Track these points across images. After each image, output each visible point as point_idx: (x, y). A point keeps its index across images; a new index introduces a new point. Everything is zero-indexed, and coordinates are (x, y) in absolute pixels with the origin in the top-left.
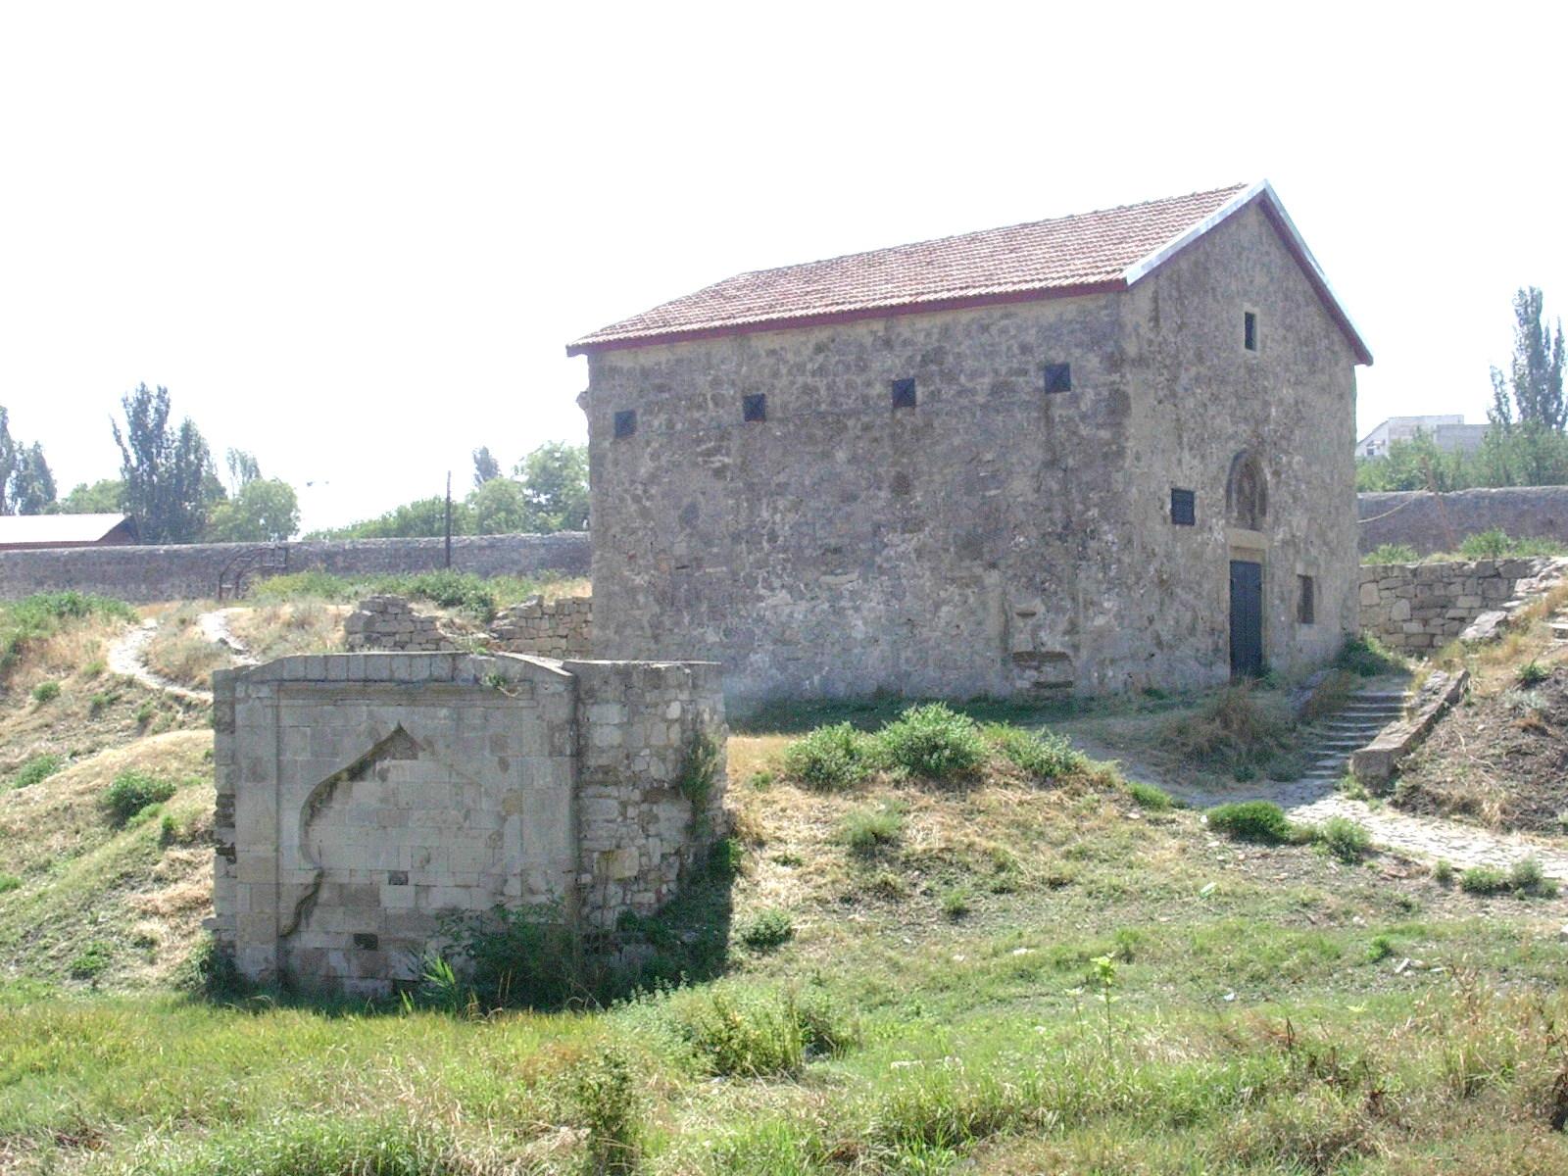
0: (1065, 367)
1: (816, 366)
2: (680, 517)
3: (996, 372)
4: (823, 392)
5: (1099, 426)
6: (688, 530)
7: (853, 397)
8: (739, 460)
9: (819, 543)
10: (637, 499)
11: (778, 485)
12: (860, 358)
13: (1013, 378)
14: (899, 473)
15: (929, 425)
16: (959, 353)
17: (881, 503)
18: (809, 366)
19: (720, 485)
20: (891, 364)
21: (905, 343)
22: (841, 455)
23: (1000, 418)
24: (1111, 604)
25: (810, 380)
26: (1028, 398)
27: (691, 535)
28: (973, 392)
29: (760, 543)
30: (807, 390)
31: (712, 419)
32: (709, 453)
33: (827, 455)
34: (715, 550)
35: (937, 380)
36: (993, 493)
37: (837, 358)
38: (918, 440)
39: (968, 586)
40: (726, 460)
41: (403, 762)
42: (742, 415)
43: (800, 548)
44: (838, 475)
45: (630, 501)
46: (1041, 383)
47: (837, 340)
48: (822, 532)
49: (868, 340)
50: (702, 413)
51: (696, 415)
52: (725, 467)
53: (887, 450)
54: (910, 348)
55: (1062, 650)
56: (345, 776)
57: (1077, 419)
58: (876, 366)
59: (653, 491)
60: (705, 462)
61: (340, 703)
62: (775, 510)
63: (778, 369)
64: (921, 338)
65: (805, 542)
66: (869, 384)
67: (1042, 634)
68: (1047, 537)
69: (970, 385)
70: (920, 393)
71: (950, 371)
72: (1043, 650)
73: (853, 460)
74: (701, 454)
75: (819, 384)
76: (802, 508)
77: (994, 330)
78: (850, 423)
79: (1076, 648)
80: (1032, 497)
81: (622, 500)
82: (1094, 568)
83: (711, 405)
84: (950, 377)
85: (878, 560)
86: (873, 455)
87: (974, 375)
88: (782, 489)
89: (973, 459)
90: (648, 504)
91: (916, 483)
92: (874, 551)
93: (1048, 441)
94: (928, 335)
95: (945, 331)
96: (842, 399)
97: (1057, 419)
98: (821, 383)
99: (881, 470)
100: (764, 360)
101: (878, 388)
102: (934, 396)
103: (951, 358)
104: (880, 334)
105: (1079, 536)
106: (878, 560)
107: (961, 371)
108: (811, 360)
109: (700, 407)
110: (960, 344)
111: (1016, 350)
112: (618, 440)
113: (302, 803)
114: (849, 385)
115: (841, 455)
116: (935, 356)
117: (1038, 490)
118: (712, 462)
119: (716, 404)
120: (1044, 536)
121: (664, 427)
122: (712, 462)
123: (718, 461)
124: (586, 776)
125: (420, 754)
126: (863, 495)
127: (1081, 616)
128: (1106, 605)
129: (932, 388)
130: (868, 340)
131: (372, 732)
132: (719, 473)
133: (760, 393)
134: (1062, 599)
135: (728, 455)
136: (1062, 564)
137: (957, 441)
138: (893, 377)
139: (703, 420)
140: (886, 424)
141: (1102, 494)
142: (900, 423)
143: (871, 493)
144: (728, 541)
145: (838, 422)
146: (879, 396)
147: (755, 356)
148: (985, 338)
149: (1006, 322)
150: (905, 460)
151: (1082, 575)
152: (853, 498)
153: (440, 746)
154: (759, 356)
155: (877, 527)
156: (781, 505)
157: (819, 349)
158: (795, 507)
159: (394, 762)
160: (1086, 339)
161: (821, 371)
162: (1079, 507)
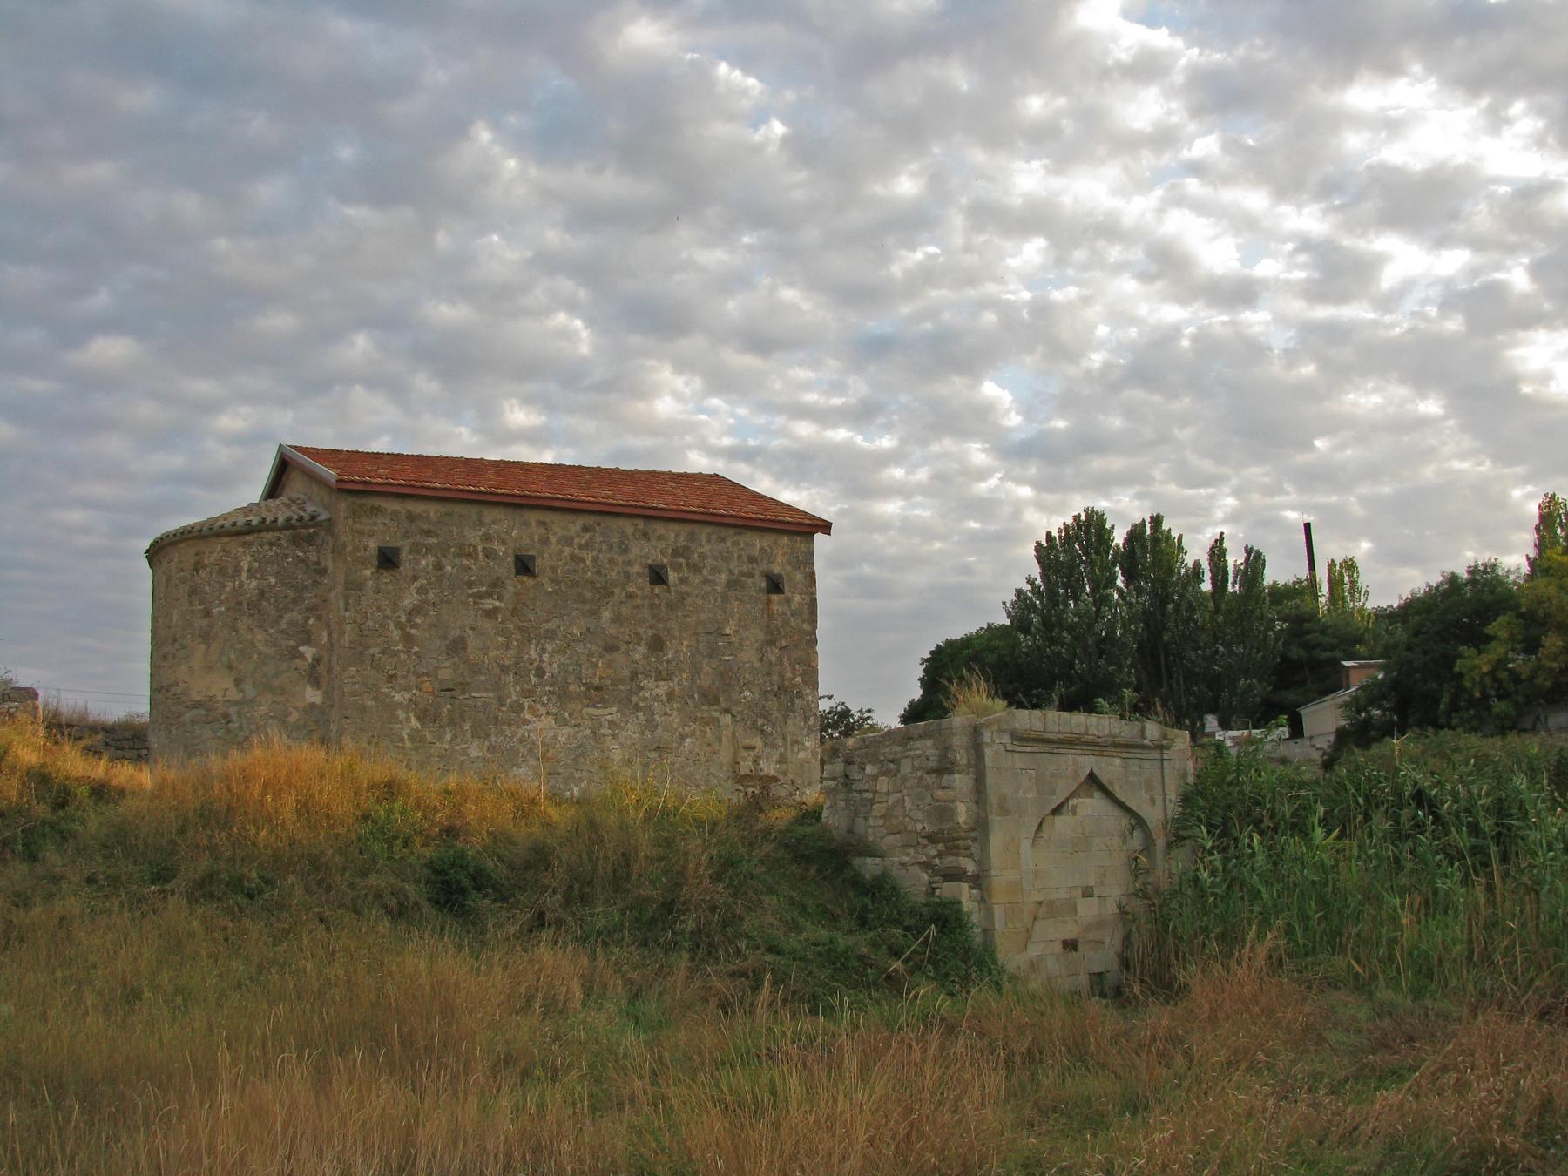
1: (583, 541)
3: (731, 572)
4: (588, 562)
7: (616, 571)
8: (510, 607)
10: (400, 626)
12: (622, 543)
18: (576, 541)
19: (488, 626)
22: (606, 615)
25: (577, 551)
28: (713, 583)
29: (528, 676)
31: (482, 568)
32: (478, 596)
33: (595, 613)
39: (707, 724)
40: (497, 604)
45: (392, 627)
46: (764, 585)
51: (465, 562)
52: (496, 609)
58: (635, 551)
63: (548, 538)
66: (629, 563)
69: (711, 578)
72: (761, 774)
73: (617, 619)
74: (471, 596)
81: (383, 625)
83: (481, 556)
84: (696, 569)
85: (635, 699)
87: (715, 570)
88: (551, 635)
90: (413, 631)
93: (768, 626)
99: (641, 630)
101: (636, 568)
102: (683, 581)
103: (696, 555)
108: (579, 536)
109: (469, 556)
112: (381, 571)
115: (606, 615)
117: (761, 660)
118: (483, 604)
122: (483, 604)
123: (489, 604)
127: (789, 752)
128: (806, 744)
132: (491, 614)
133: (530, 553)
135: (500, 598)
138: (649, 561)
146: (638, 573)
150: (660, 626)
151: (789, 722)
156: (549, 647)
159: (1080, 800)
161: (587, 546)
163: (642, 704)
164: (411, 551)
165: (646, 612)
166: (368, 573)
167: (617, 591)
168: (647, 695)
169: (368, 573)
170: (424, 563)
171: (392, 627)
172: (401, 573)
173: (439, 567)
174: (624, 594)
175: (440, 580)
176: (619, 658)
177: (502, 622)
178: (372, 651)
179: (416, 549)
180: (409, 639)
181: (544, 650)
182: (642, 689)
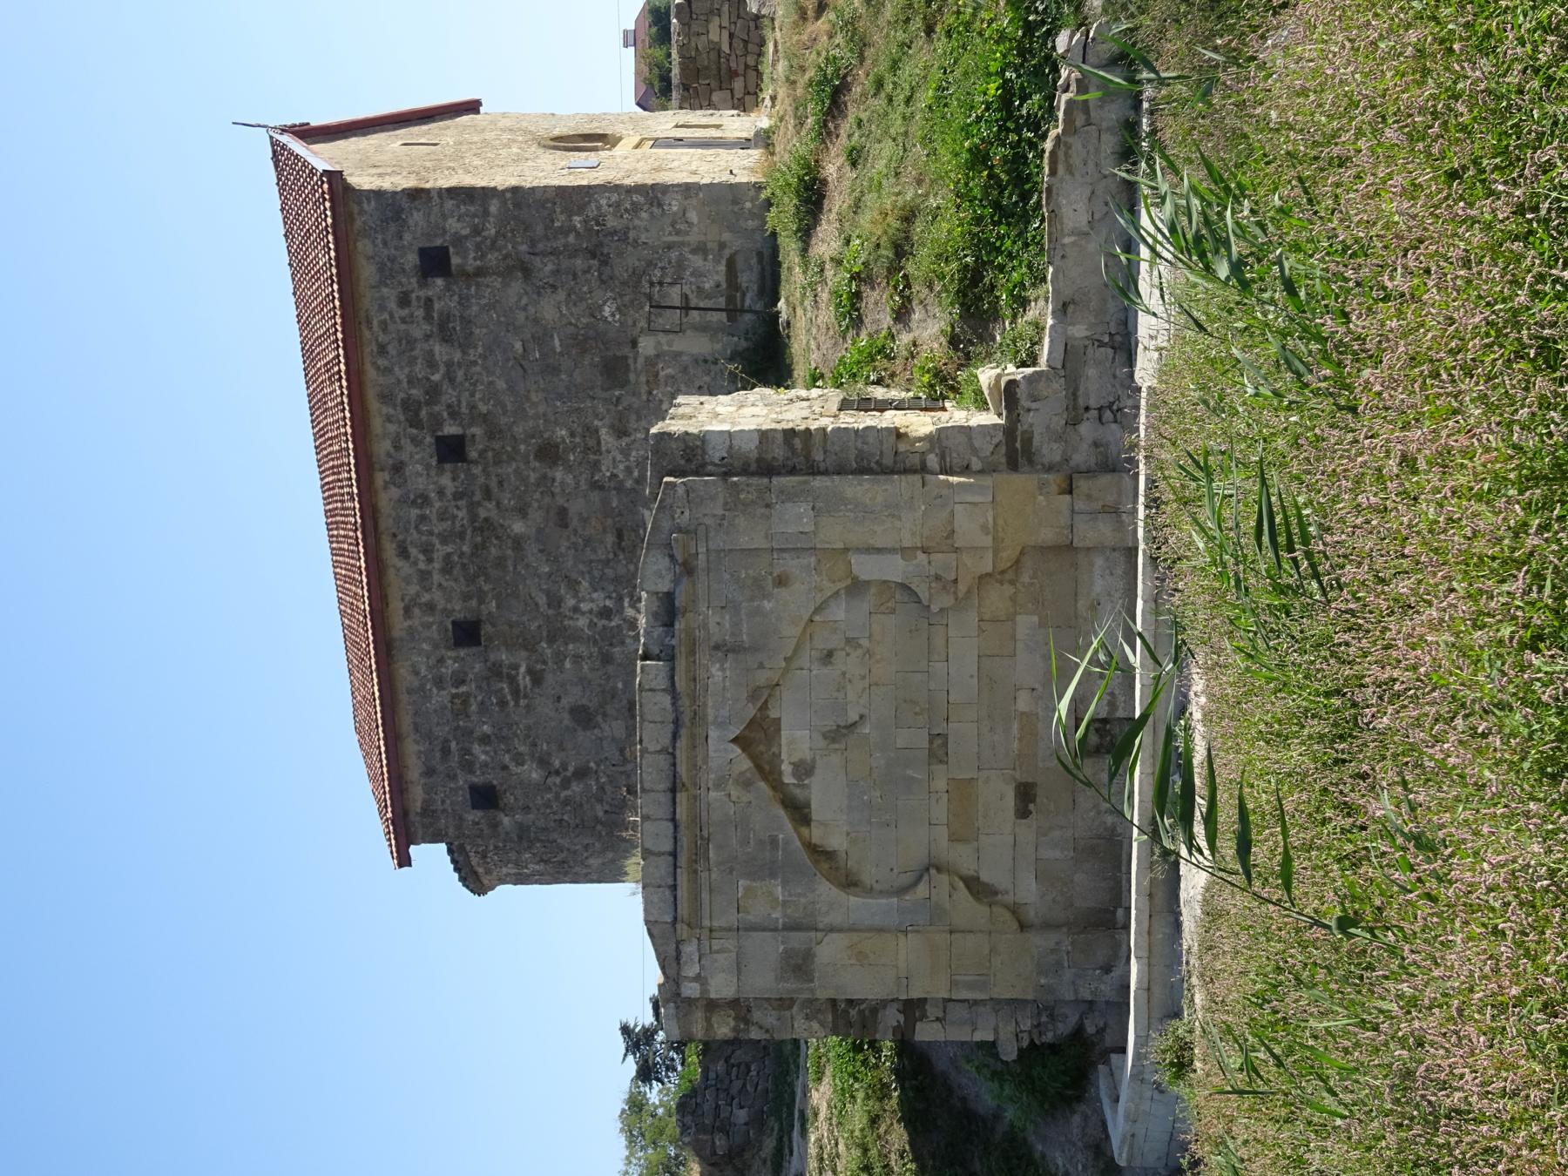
0: (424, 253)
1: (422, 557)
2: (585, 729)
3: (428, 337)
4: (449, 549)
5: (486, 213)
6: (599, 718)
7: (455, 511)
8: (524, 654)
9: (611, 556)
10: (566, 784)
11: (549, 606)
12: (414, 502)
13: (435, 315)
14: (536, 456)
15: (485, 418)
16: (409, 382)
17: (569, 479)
18: (422, 566)
19: (550, 679)
20: (419, 460)
21: (397, 447)
22: (518, 527)
23: (478, 331)
24: (674, 203)
25: (437, 565)
26: (456, 298)
27: (605, 715)
28: (449, 364)
30: (447, 569)
31: (479, 687)
32: (516, 693)
33: (518, 543)
34: (620, 685)
35: (437, 408)
36: (557, 342)
37: (413, 531)
38: (501, 431)
39: (657, 375)
40: (523, 669)
41: (784, 741)
42: (474, 649)
43: (616, 580)
44: (540, 531)
45: (568, 793)
46: (440, 282)
47: (394, 530)
48: (600, 552)
49: (394, 492)
50: (472, 700)
51: (474, 708)
52: (530, 671)
53: (510, 470)
54: (402, 442)
55: (724, 262)
56: (804, 831)
57: (478, 239)
58: (420, 484)
59: (557, 763)
60: (526, 696)
61: (705, 833)
62: (576, 609)
63: (426, 605)
64: (392, 428)
65: (609, 572)
66: (441, 493)
67: (707, 286)
68: (604, 277)
69: (442, 369)
70: (451, 429)
71: (427, 393)
72: (724, 285)
73: (522, 512)
74: (517, 704)
75: (441, 554)
76: (574, 576)
77: (382, 338)
78: (483, 513)
79: (722, 246)
80: (561, 295)
81: (566, 802)
82: (637, 222)
83: (463, 689)
84: (433, 392)
85: (629, 484)
86: (517, 488)
87: (432, 364)
88: (555, 602)
89: (521, 366)
90: (571, 769)
91: (546, 435)
92: (620, 488)
93: (499, 274)
94: (389, 419)
95: (386, 398)
96: (458, 524)
97: (478, 262)
98: (441, 550)
99: (533, 477)
100: (416, 622)
101: (445, 480)
102: (454, 414)
103: (414, 392)
104: (388, 478)
105: (601, 238)
106: (629, 484)
107: (428, 379)
108: (415, 563)
109: (465, 703)
110: (399, 381)
111: (405, 312)
112: (501, 805)
113: (842, 894)
114: (443, 516)
115: (518, 527)
116: (411, 407)
117: (555, 288)
118: (525, 687)
119: (463, 682)
120: (603, 282)
121: (488, 748)
122: (525, 687)
123: (524, 681)
124: (799, 461)
125: (773, 714)
126: (560, 501)
127: (687, 239)
128: (675, 208)
129: (445, 414)
130: (394, 492)
131: (747, 784)
132: (537, 678)
133: (450, 627)
134: (670, 262)
135: (516, 667)
136: (632, 260)
137: (501, 385)
138: (434, 462)
139: (480, 698)
140: (483, 471)
141: (558, 210)
142: (482, 453)
143: (557, 490)
144: (611, 669)
145: (481, 529)
146: (454, 479)
147: (411, 631)
148: (392, 350)
149: (375, 323)
150: (522, 447)
151: (643, 238)
152: (562, 513)
153: (762, 677)
154: (410, 627)
155: (596, 486)
156: (571, 602)
157: (403, 553)
158: (573, 585)
159: (784, 756)
160: (393, 228)
161: (427, 550)
162: (571, 238)
163: (636, 474)
164: (472, 772)
165: (509, 469)
166: (506, 820)
167: (483, 513)
168: (621, 467)
169: (506, 820)
170: (483, 757)
171: (568, 793)
172: (501, 785)
173: (485, 740)
174: (487, 504)
175: (503, 739)
176: (576, 507)
177: (545, 663)
178: (600, 814)
179: (468, 766)
180: (582, 773)
181: (576, 609)
182: (614, 476)
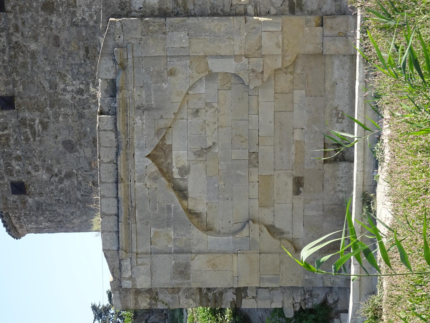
2: (70, 152)
6: (78, 147)
8: (38, 113)
10: (61, 181)
14: (42, 8)
17: (60, 21)
19: (52, 126)
22: (33, 46)
27: (81, 145)
29: (84, 100)
32: (34, 134)
33: (33, 55)
34: (88, 129)
40: (37, 121)
41: (174, 157)
42: (12, 111)
43: (86, 74)
44: (45, 48)
45: (63, 185)
50: (11, 137)
51: (12, 142)
52: (41, 122)
53: (28, 16)
56: (185, 203)
59: (56, 170)
60: (39, 136)
61: (133, 204)
62: (64, 90)
65: (82, 70)
73: (35, 38)
74: (34, 140)
76: (63, 72)
78: (14, 39)
81: (61, 190)
83: (6, 132)
85: (91, 23)
88: (53, 86)
90: (63, 173)
99: (41, 20)
106: (91, 23)
109: (7, 139)
112: (28, 192)
118: (39, 131)
119: (6, 128)
121: (20, 163)
122: (39, 131)
123: (38, 127)
124: (181, 9)
125: (168, 142)
126: (55, 32)
131: (155, 179)
132: (45, 126)
135: (34, 120)
139: (15, 137)
142: (13, 7)
143: (54, 27)
144: (83, 121)
145: (14, 48)
153: (162, 123)
155: (74, 24)
156: (62, 86)
158: (63, 77)
159: (174, 164)
163: (95, 18)
164: (12, 175)
165: (28, 16)
166: (30, 200)
167: (14, 39)
168: (87, 14)
169: (30, 200)
170: (17, 167)
171: (63, 185)
172: (27, 182)
173: (18, 158)
174: (16, 34)
175: (28, 158)
176: (64, 35)
177: (49, 118)
178: (79, 196)
179: (10, 172)
180: (69, 175)
181: (64, 90)
182: (83, 19)
